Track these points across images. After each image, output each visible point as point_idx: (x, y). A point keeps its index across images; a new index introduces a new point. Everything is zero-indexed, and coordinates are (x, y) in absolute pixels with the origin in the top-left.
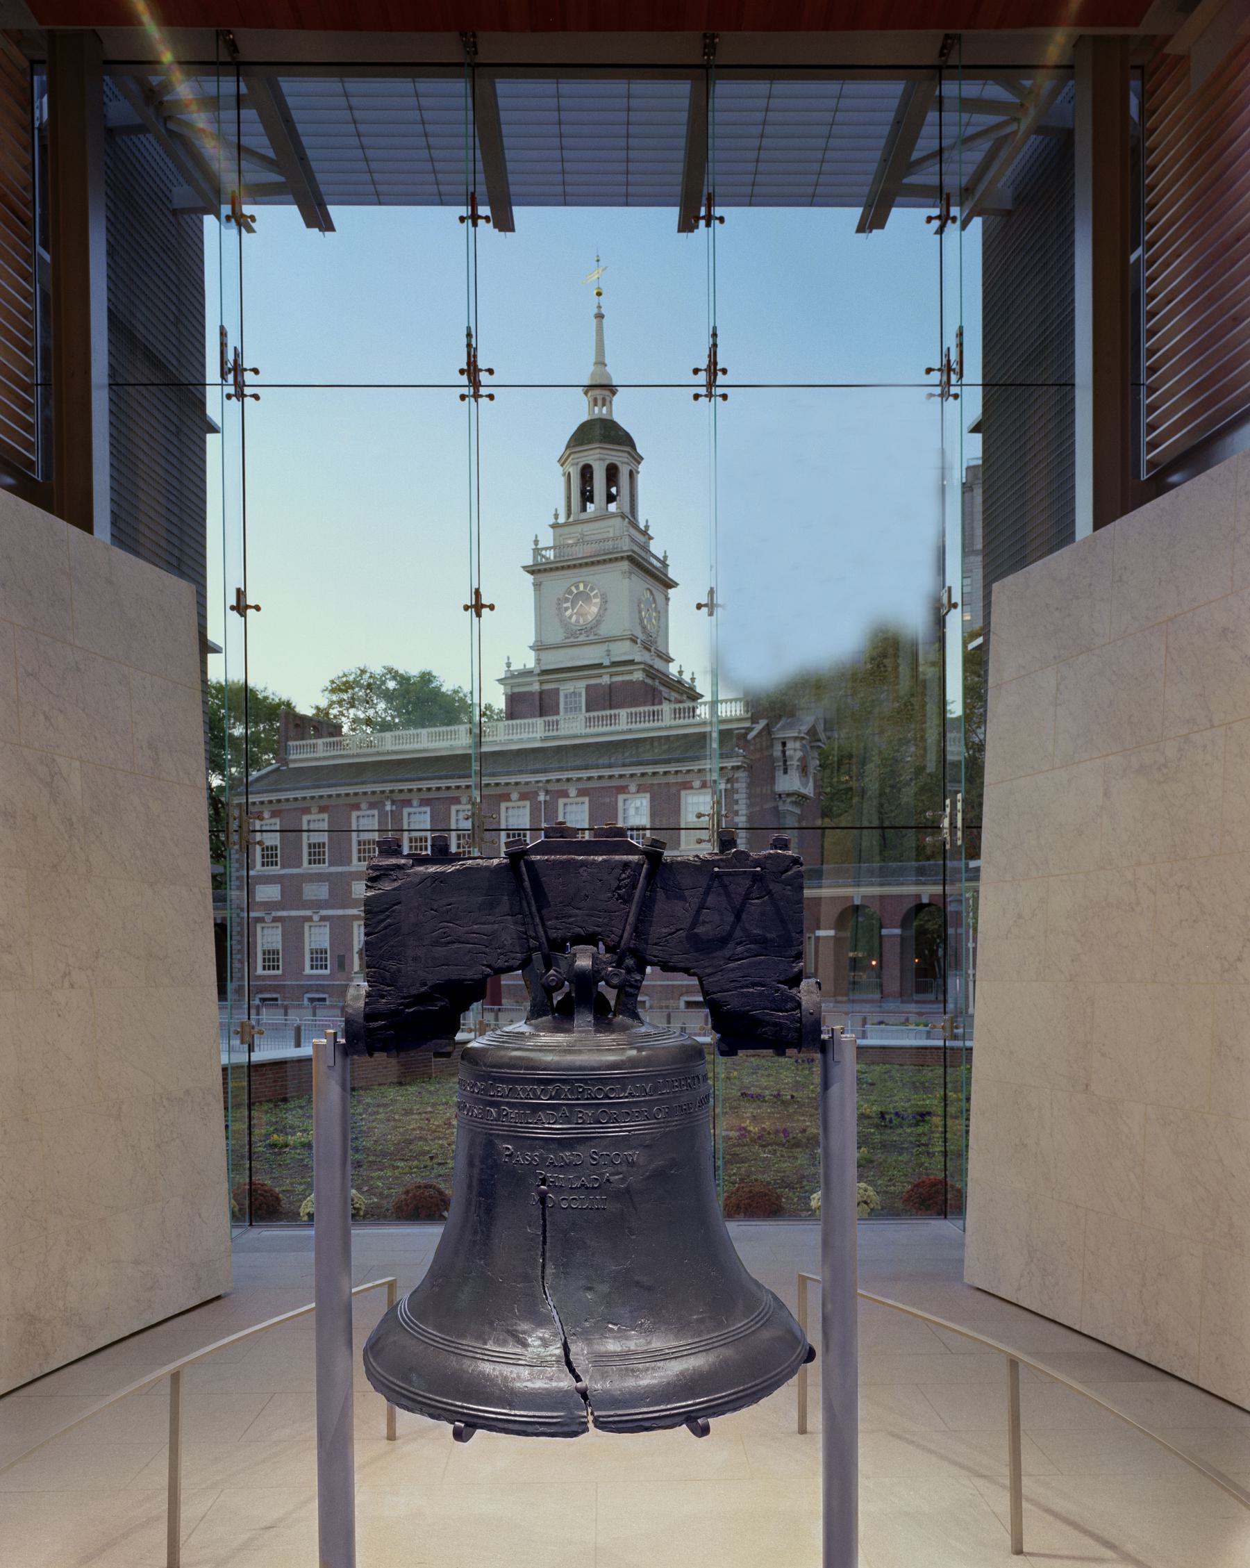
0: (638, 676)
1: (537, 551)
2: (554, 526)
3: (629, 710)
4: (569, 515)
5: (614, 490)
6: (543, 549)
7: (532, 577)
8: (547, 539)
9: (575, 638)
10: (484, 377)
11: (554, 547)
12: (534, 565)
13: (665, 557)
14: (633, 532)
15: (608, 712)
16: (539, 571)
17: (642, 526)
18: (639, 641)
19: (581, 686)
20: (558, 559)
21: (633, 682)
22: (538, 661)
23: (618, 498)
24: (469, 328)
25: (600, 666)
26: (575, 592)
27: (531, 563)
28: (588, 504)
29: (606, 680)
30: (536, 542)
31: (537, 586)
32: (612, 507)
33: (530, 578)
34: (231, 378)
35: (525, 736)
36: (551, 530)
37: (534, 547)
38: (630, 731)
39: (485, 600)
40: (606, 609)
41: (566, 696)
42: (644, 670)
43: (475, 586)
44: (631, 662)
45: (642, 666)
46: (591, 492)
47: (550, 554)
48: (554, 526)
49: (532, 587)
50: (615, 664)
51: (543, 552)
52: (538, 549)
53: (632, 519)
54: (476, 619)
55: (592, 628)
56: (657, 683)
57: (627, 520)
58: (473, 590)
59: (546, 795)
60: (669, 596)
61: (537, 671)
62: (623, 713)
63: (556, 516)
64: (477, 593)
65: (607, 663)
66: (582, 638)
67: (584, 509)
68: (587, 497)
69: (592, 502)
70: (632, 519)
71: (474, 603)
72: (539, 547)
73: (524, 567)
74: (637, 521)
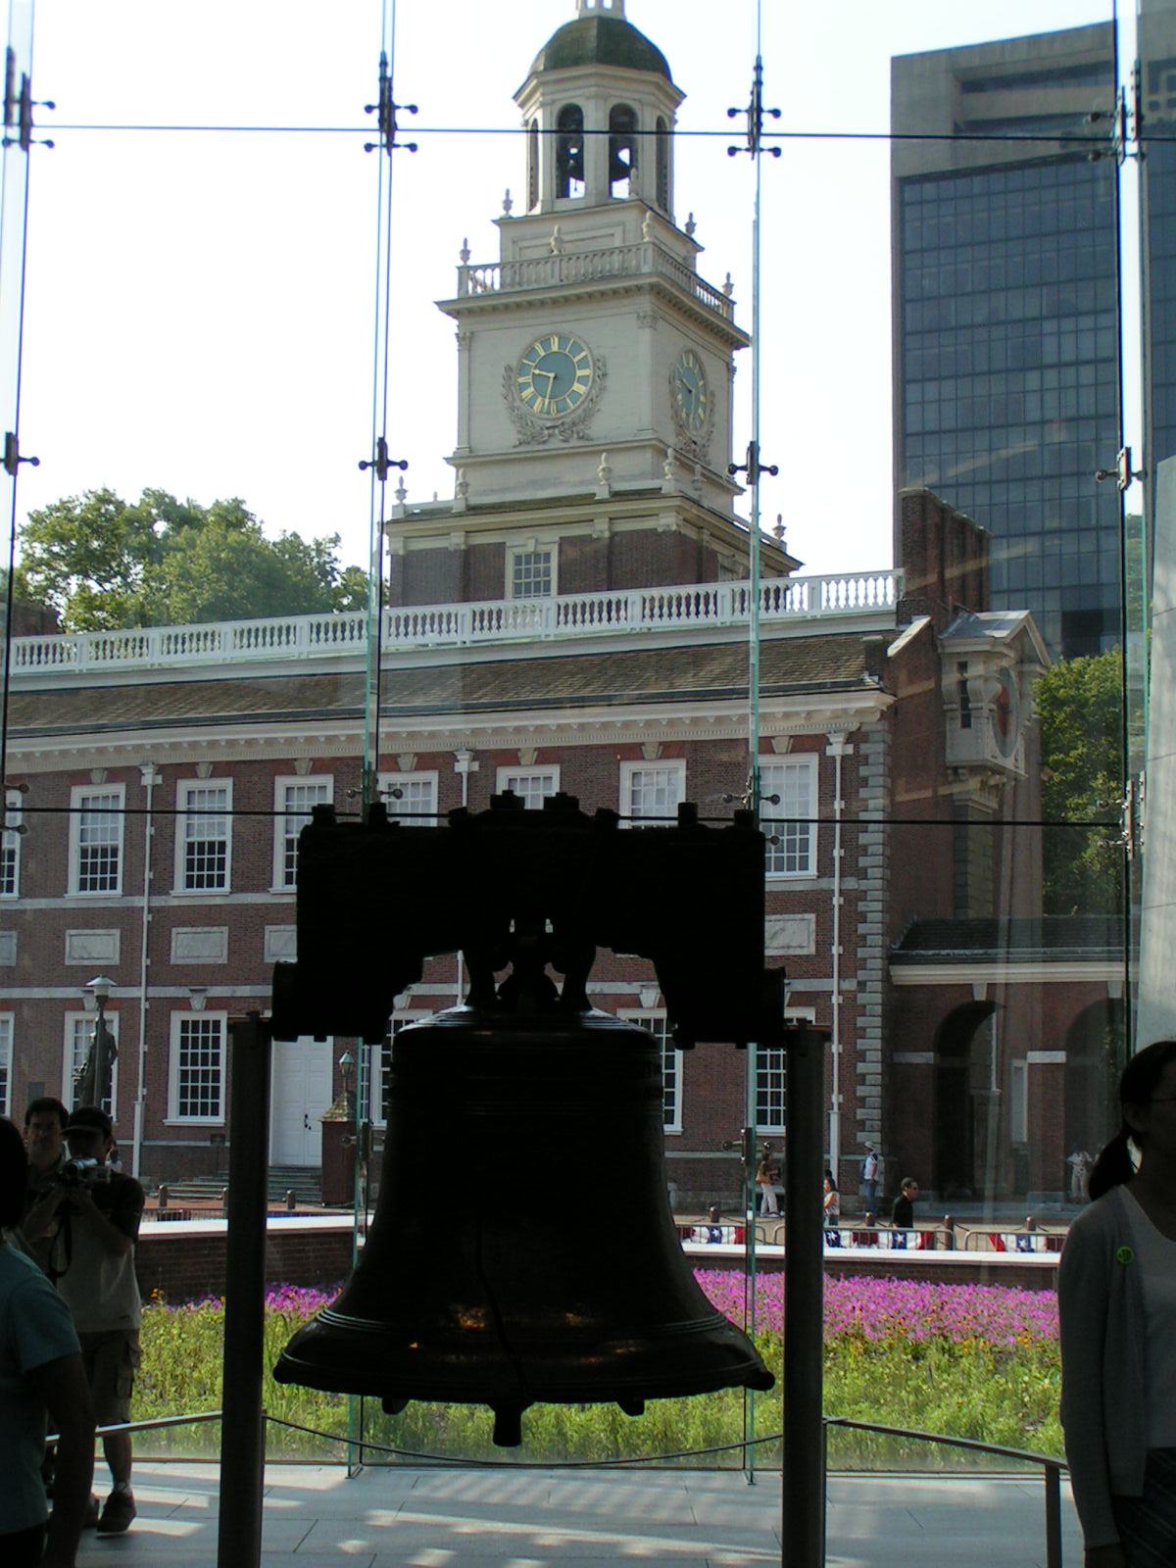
0: (668, 521)
1: (466, 272)
2: (504, 223)
3: (648, 593)
4: (532, 204)
5: (624, 155)
6: (476, 268)
7: (455, 322)
8: (488, 248)
9: (540, 443)
10: (402, 118)
11: (502, 265)
12: (459, 300)
13: (729, 286)
14: (664, 235)
15: (605, 596)
16: (470, 311)
17: (681, 224)
18: (670, 451)
19: (548, 541)
20: (508, 289)
21: (659, 535)
22: (463, 487)
23: (633, 172)
24: (383, 55)
25: (588, 499)
26: (543, 354)
27: (454, 295)
28: (572, 181)
29: (601, 529)
30: (465, 254)
31: (466, 341)
32: (621, 189)
33: (451, 325)
34: (16, 110)
35: (432, 638)
36: (496, 229)
37: (461, 263)
38: (649, 634)
39: (393, 455)
40: (603, 389)
41: (518, 559)
42: (679, 510)
43: (379, 434)
44: (654, 493)
45: (677, 502)
46: (579, 157)
47: (493, 279)
48: (504, 223)
49: (454, 344)
50: (617, 496)
51: (479, 274)
52: (469, 268)
53: (661, 212)
54: (378, 483)
55: (574, 424)
56: (706, 537)
57: (649, 214)
58: (377, 440)
59: (474, 759)
60: (735, 364)
61: (460, 507)
62: (634, 596)
63: (508, 204)
64: (382, 445)
65: (602, 493)
66: (556, 443)
67: (563, 191)
68: (568, 167)
69: (580, 177)
70: (661, 212)
71: (376, 458)
72: (470, 263)
73: (437, 303)
74: (671, 215)
